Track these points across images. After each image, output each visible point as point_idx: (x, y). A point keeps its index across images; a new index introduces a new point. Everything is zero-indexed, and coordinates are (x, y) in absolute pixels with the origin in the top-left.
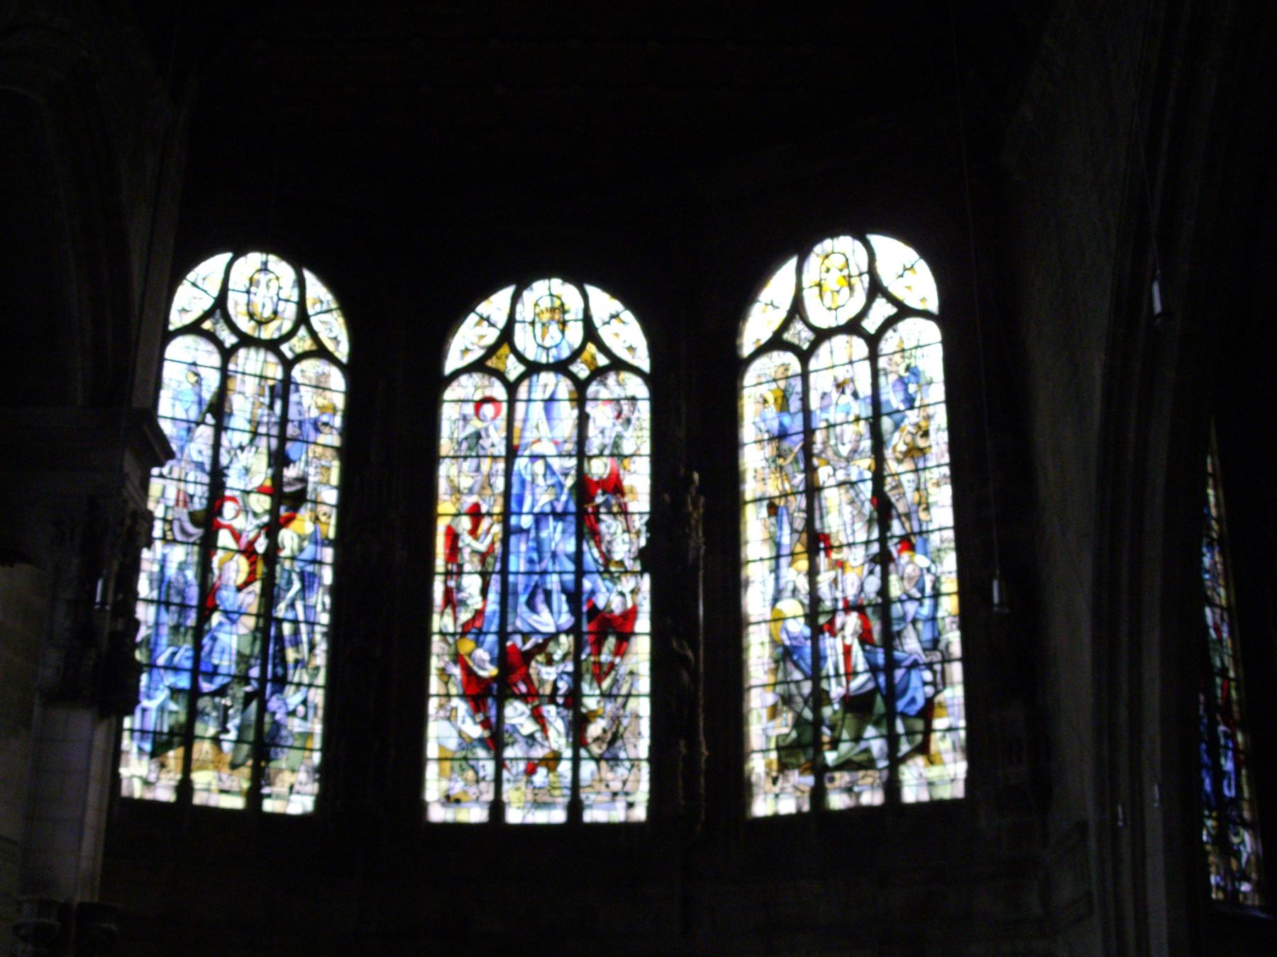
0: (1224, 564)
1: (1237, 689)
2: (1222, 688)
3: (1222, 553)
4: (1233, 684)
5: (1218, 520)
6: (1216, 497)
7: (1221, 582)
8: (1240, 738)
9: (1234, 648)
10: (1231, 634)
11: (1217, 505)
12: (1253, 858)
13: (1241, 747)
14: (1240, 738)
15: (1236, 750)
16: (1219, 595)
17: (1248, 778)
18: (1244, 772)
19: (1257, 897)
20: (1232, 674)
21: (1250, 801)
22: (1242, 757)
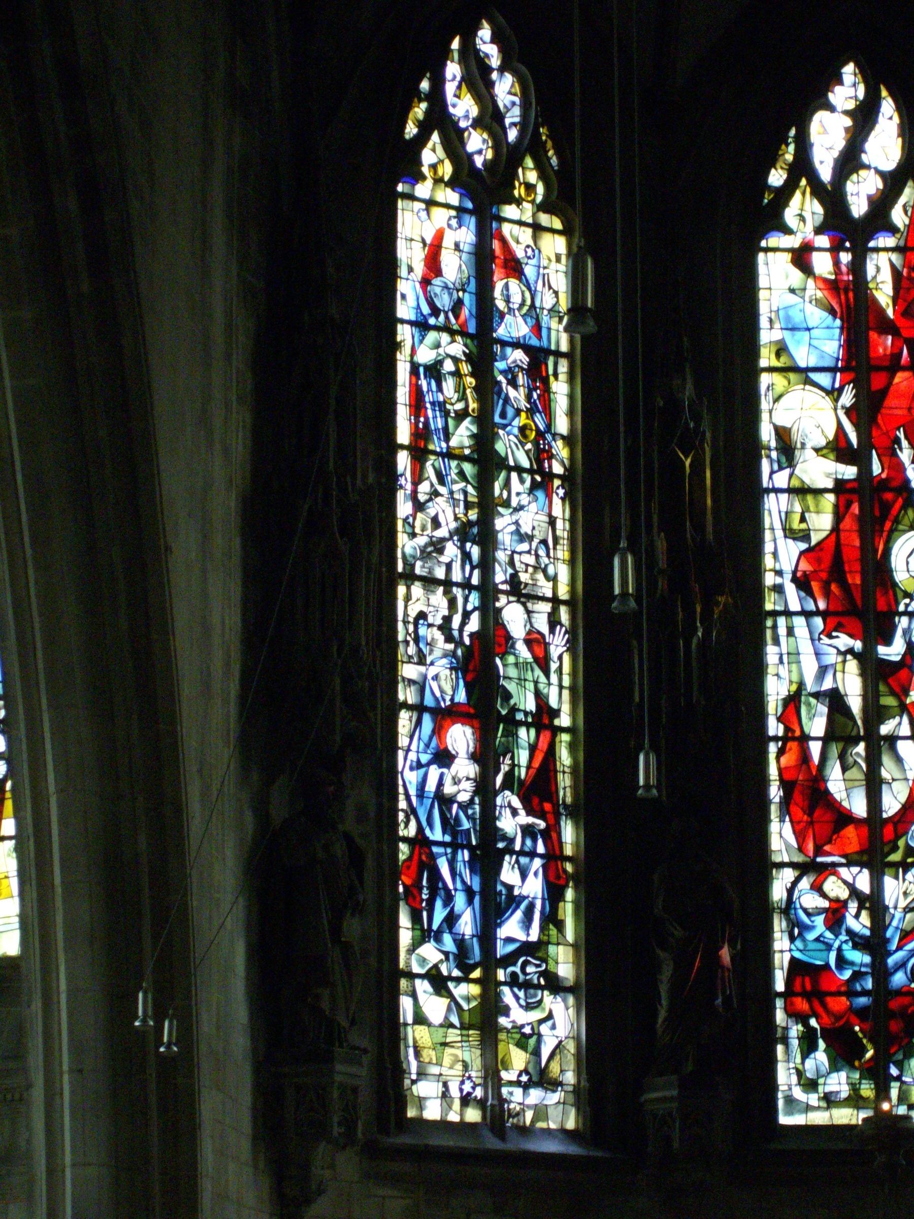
0: (572, 520)
1: (572, 747)
2: (533, 749)
3: (569, 497)
4: (565, 737)
5: (568, 440)
6: (571, 397)
7: (563, 552)
8: (568, 833)
9: (574, 674)
10: (571, 647)
11: (571, 413)
12: (571, 1046)
13: (568, 851)
14: (568, 833)
15: (554, 857)
16: (554, 579)
17: (576, 903)
18: (570, 894)
19: (573, 1113)
20: (564, 720)
21: (575, 946)
22: (569, 867)
